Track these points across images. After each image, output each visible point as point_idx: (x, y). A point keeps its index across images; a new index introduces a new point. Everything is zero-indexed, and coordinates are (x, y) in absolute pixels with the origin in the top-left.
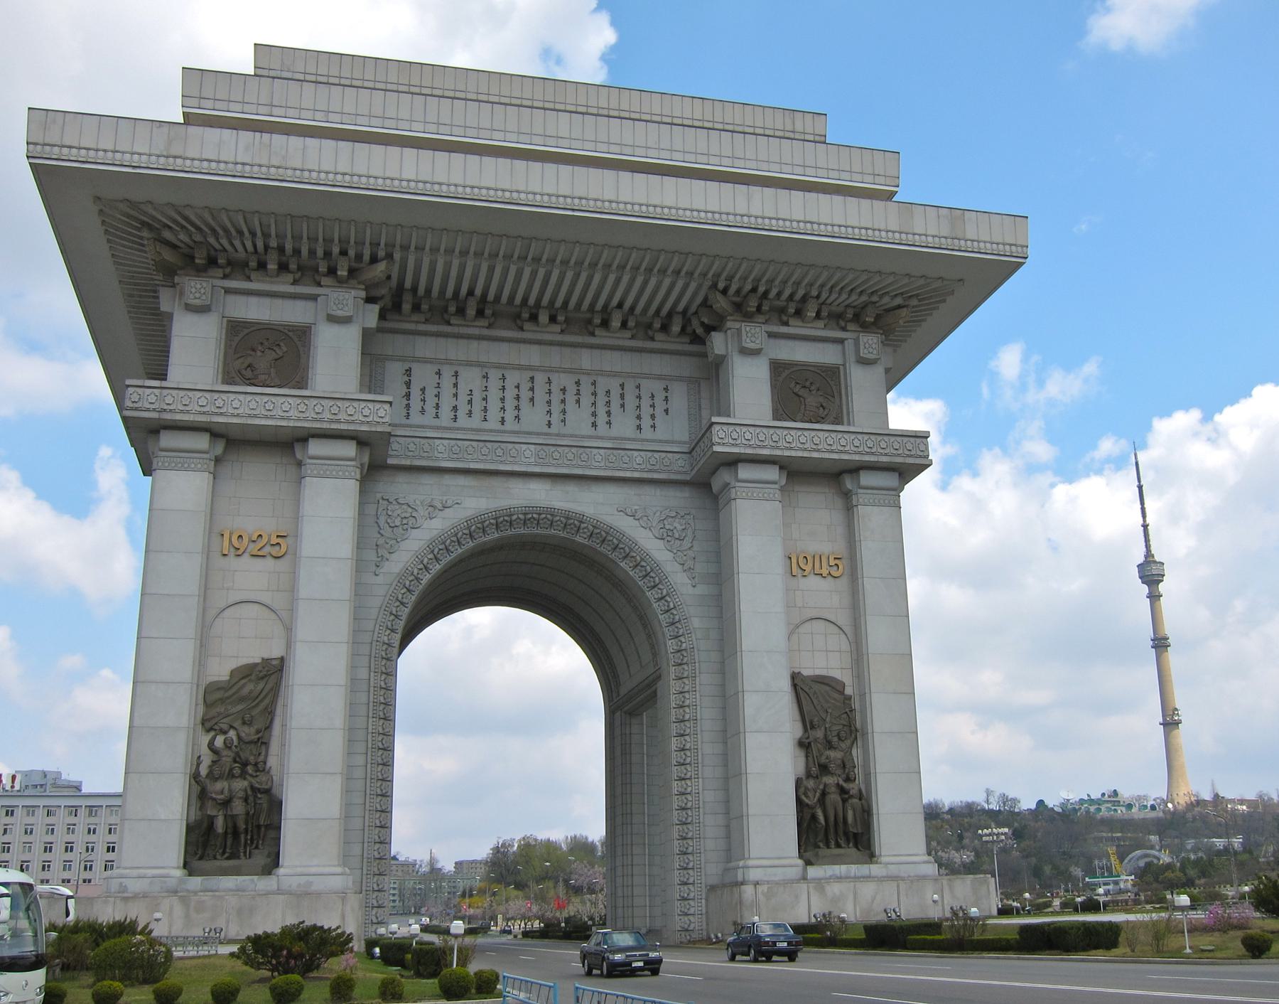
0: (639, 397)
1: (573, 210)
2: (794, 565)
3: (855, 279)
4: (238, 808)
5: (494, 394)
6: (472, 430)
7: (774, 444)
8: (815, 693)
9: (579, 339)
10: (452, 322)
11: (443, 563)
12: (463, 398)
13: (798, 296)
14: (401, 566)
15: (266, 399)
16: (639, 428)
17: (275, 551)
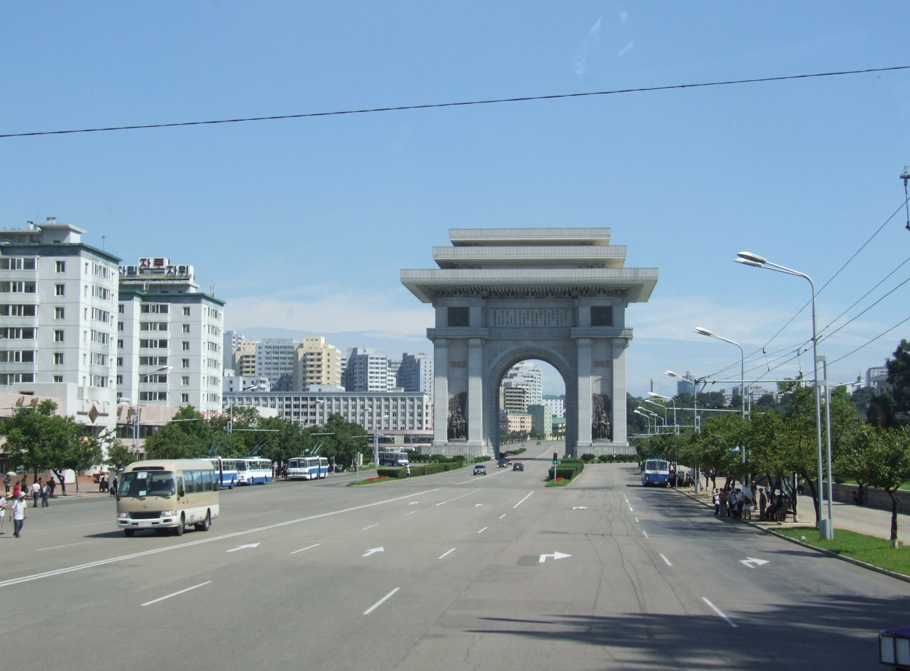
0: (558, 315)
5: (518, 317)
12: (510, 319)
16: (558, 324)
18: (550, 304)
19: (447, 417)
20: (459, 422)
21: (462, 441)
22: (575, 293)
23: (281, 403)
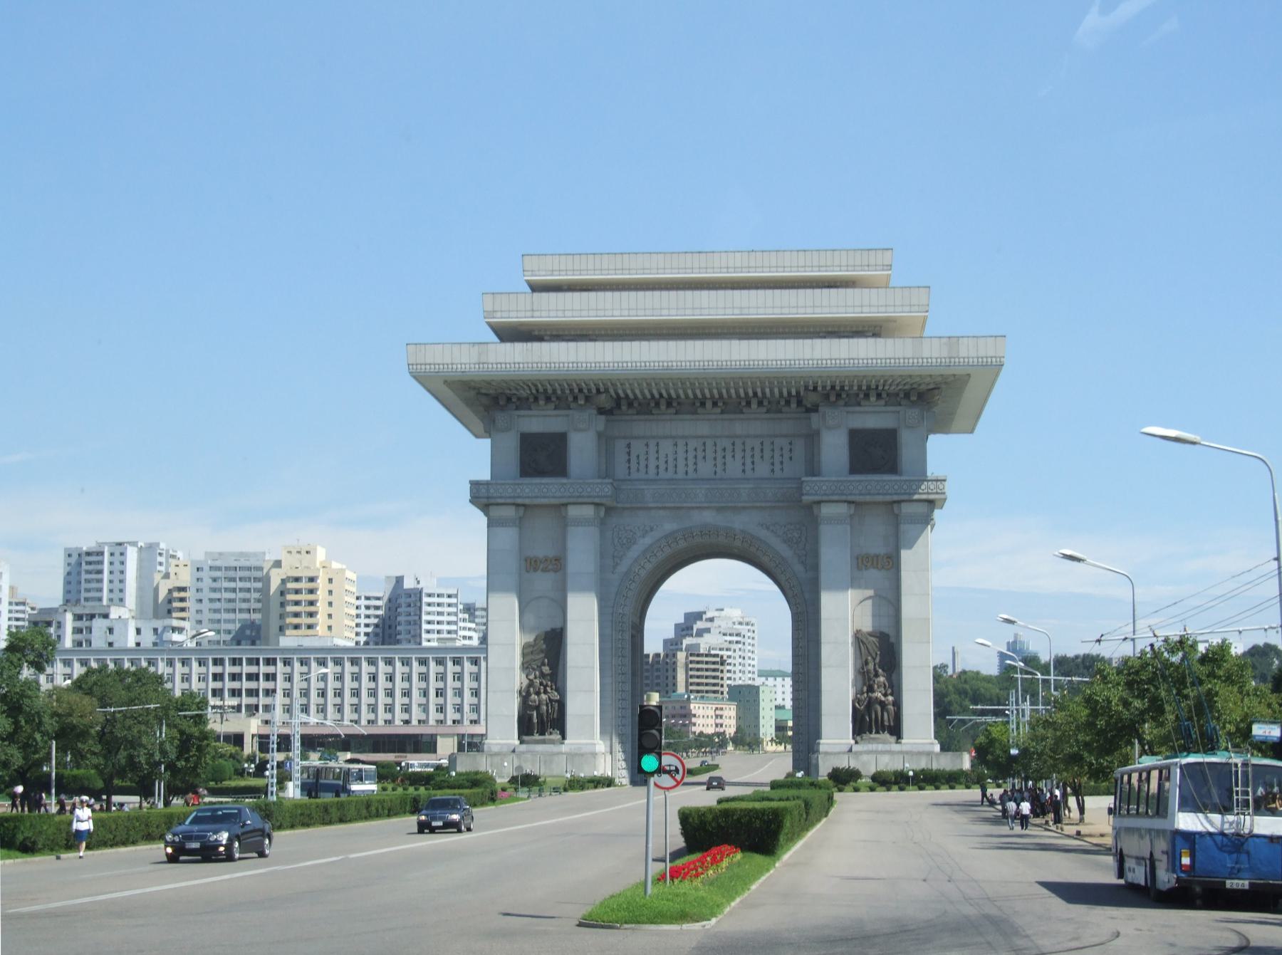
0: (773, 450)
2: (860, 565)
5: (681, 455)
9: (732, 416)
10: (653, 412)
12: (662, 459)
18: (753, 426)
19: (517, 687)
20: (544, 697)
21: (552, 742)
22: (812, 398)
23: (203, 669)
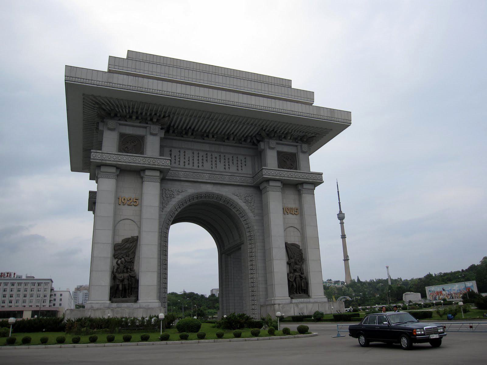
0: (238, 161)
1: (226, 104)
3: (298, 128)
4: (126, 282)
5: (196, 158)
6: (190, 169)
7: (280, 175)
8: (291, 248)
10: (184, 136)
11: (181, 208)
12: (187, 159)
13: (285, 133)
14: (170, 209)
15: (134, 157)
16: (238, 169)
17: (135, 204)
